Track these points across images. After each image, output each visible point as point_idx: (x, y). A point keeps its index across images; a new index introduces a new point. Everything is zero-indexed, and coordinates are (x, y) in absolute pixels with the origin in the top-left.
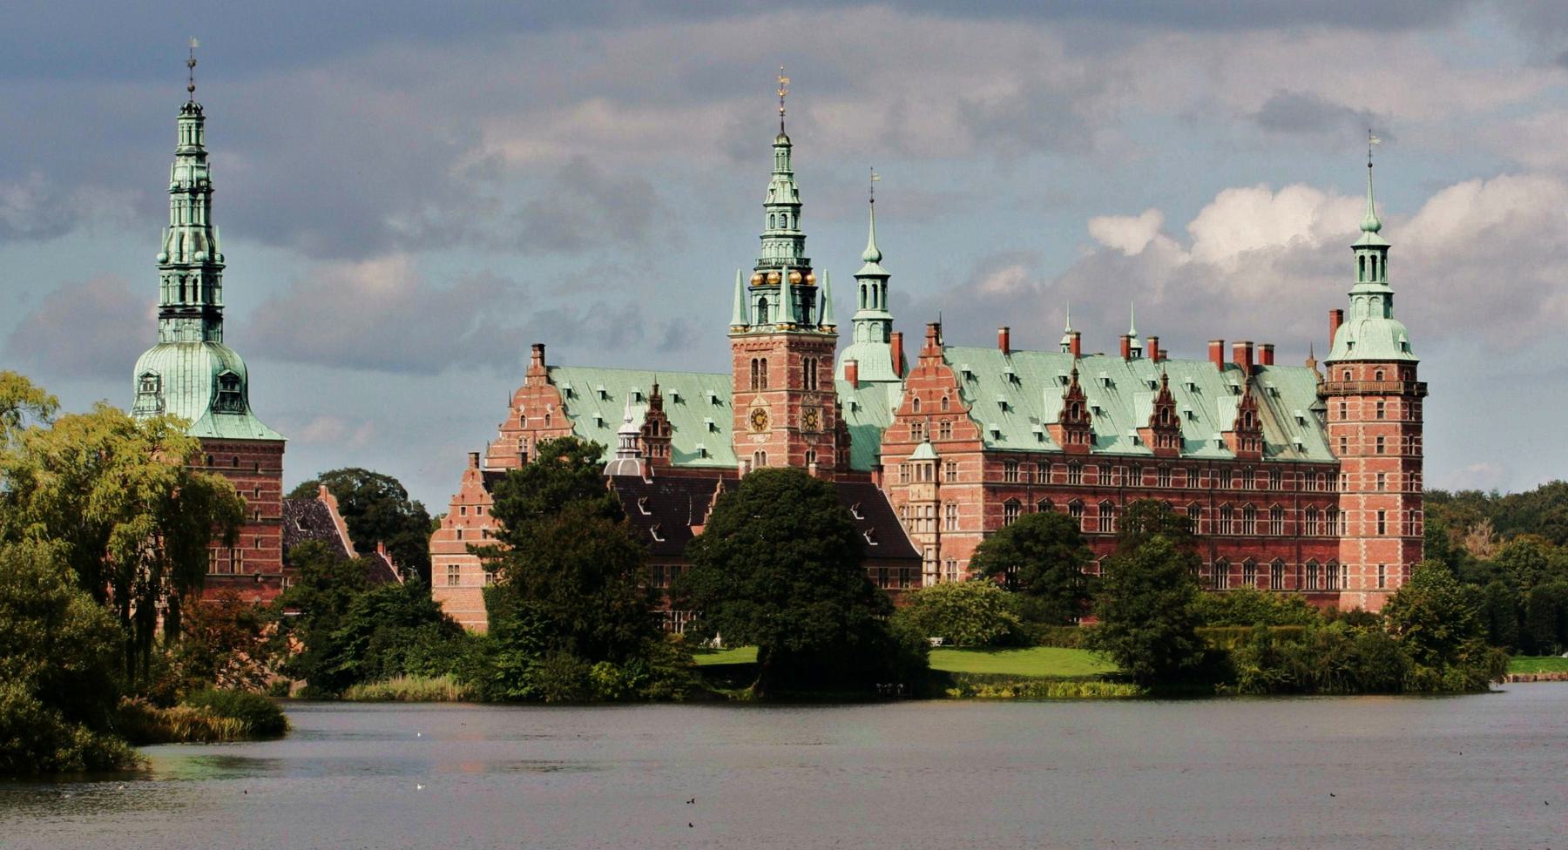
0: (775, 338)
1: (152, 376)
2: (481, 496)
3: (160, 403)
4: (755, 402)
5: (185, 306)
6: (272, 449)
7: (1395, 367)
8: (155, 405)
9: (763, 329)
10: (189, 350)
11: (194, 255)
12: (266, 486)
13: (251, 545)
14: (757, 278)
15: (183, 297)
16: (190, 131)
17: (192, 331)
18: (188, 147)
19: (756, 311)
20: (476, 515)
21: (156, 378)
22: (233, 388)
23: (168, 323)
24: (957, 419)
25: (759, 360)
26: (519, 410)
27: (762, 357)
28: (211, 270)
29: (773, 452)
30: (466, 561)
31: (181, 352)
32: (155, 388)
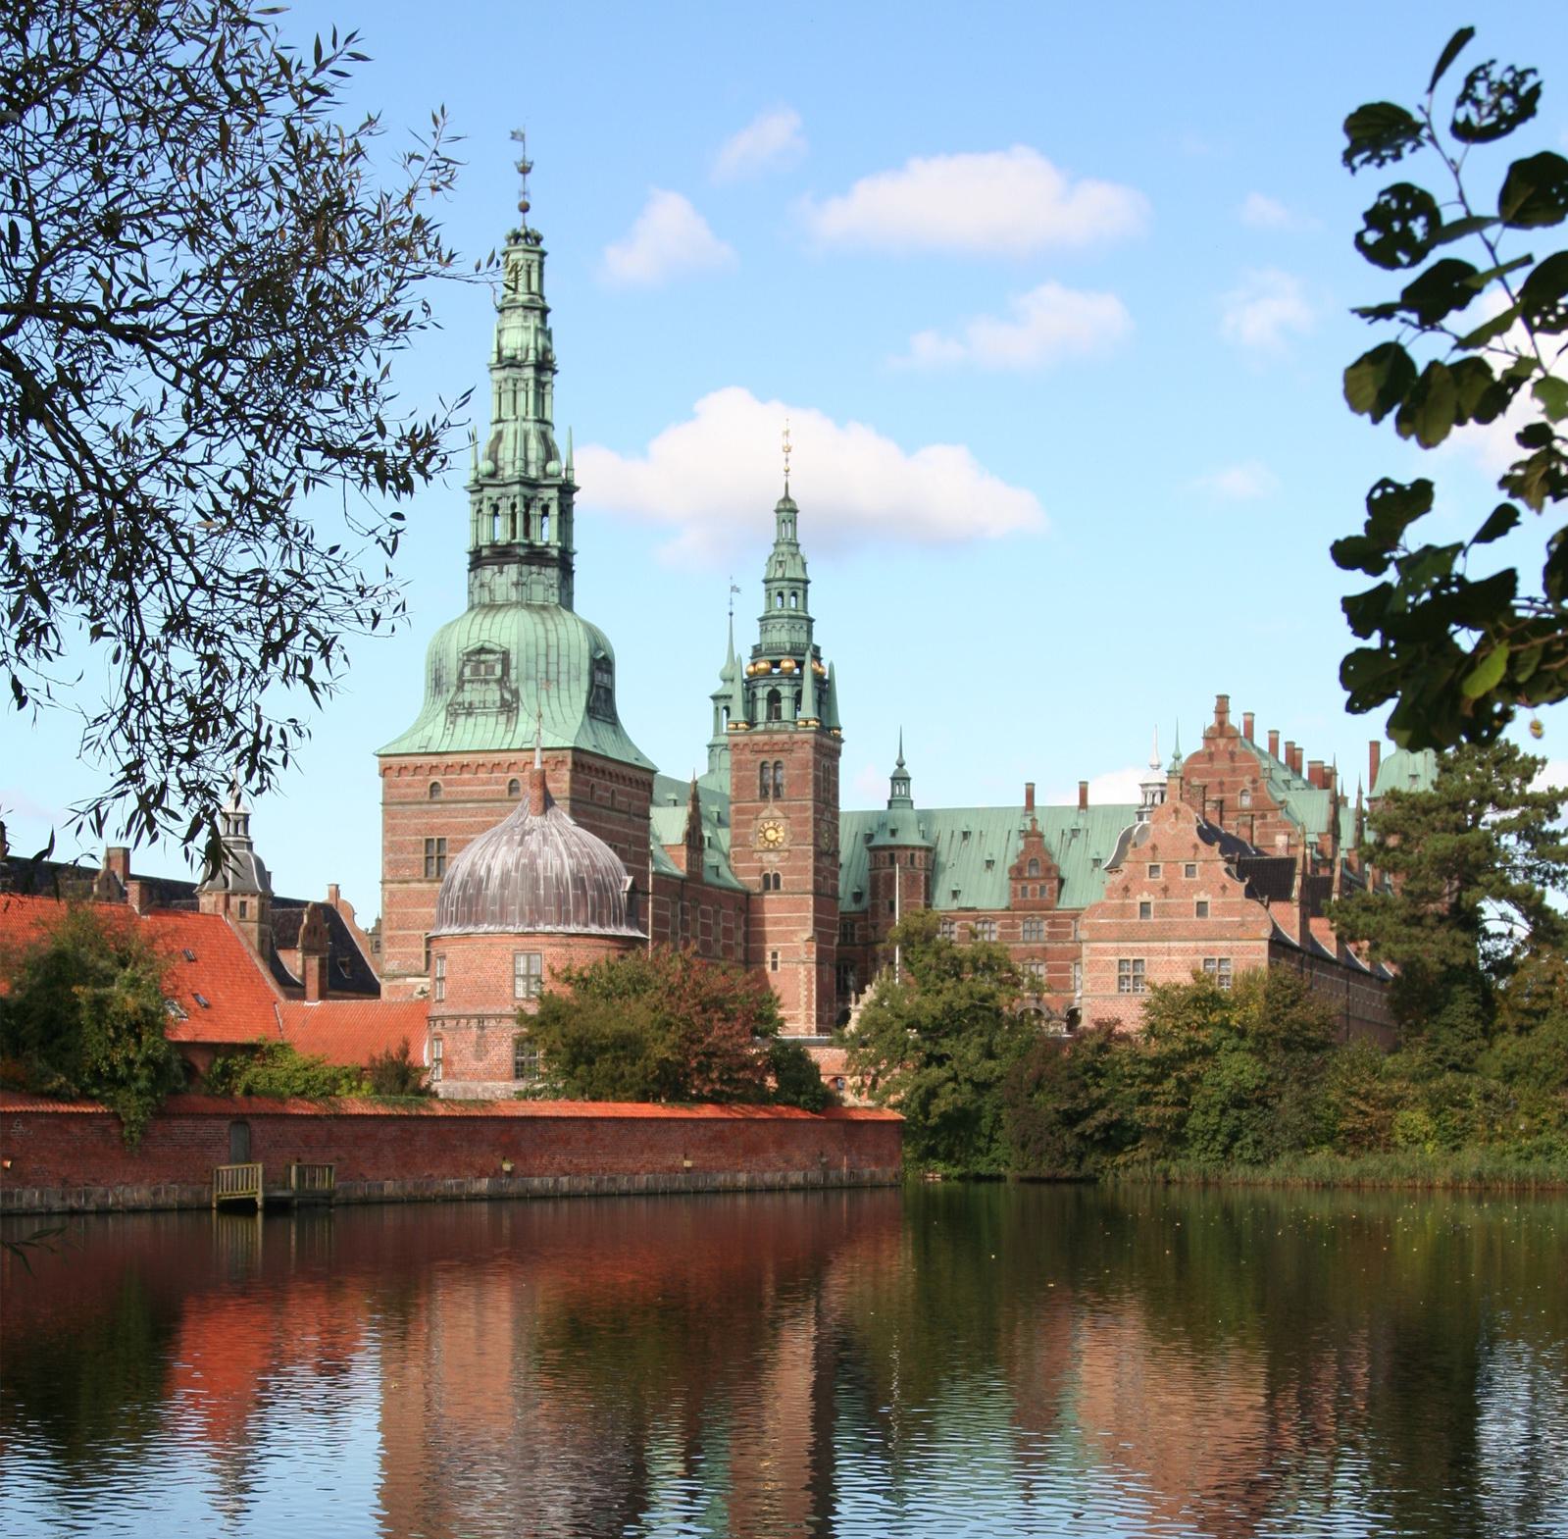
0: (797, 737)
2: (1196, 847)
3: (507, 696)
4: (765, 814)
5: (531, 546)
8: (497, 697)
9: (776, 726)
10: (546, 615)
11: (544, 468)
16: (529, 273)
17: (541, 587)
18: (527, 297)
20: (1184, 878)
23: (501, 572)
24: (1264, 817)
29: (791, 874)
30: (1160, 953)
31: (537, 618)
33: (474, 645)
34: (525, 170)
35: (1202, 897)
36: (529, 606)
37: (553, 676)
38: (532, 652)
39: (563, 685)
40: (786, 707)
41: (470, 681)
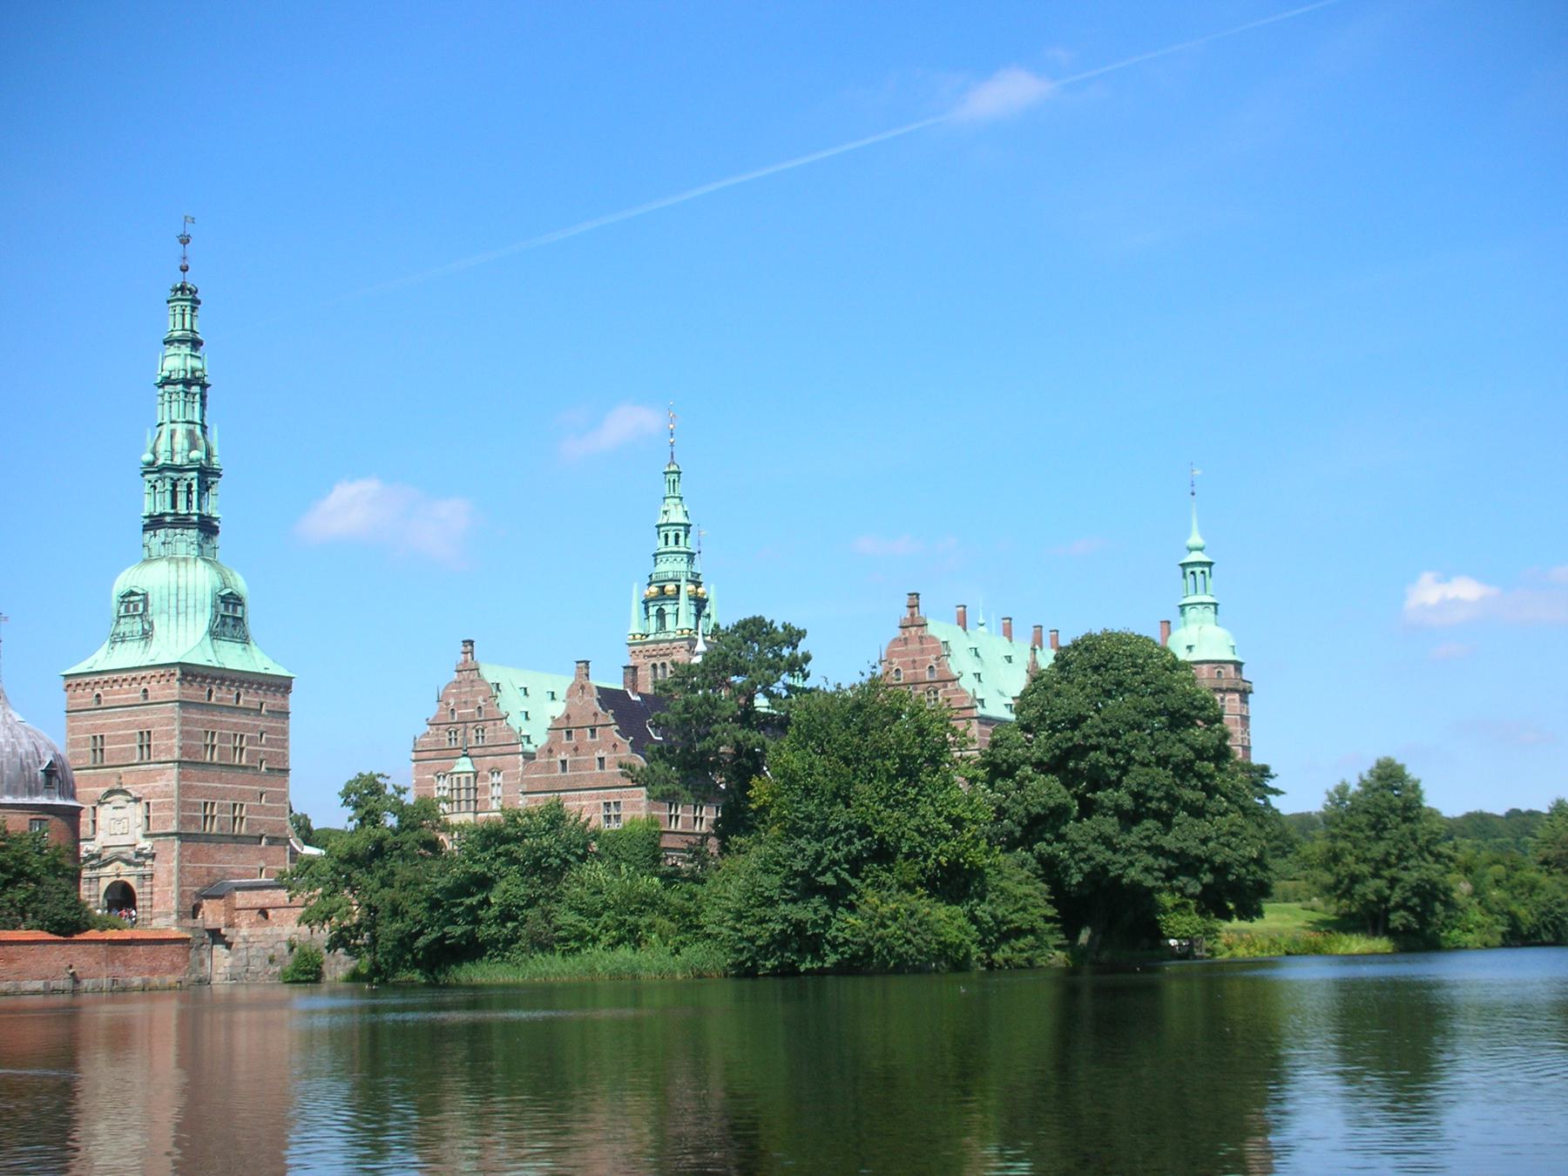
0: (675, 644)
1: (137, 594)
2: (596, 714)
3: (146, 627)
5: (176, 514)
6: (278, 687)
7: (1231, 668)
8: (140, 628)
10: (182, 564)
12: (271, 730)
13: (254, 799)
14: (654, 589)
15: (174, 505)
16: (183, 315)
17: (184, 544)
18: (180, 333)
19: (653, 620)
21: (141, 597)
22: (235, 610)
23: (155, 535)
24: (946, 686)
25: (659, 665)
26: (448, 704)
27: (661, 661)
28: (207, 474)
30: (574, 799)
31: (173, 566)
32: (141, 606)
33: (126, 590)
34: (185, 241)
35: (601, 754)
36: (170, 560)
37: (182, 609)
38: (165, 592)
39: (191, 616)
40: (670, 620)
41: (124, 617)
